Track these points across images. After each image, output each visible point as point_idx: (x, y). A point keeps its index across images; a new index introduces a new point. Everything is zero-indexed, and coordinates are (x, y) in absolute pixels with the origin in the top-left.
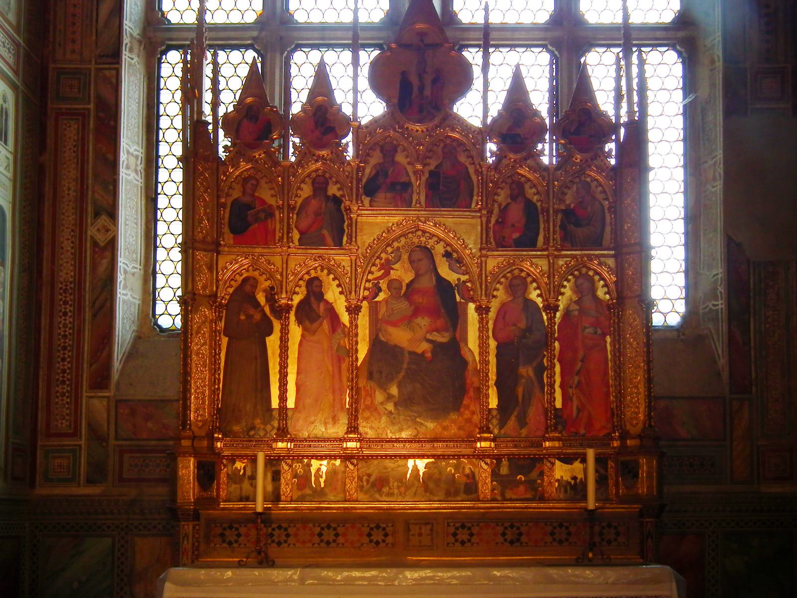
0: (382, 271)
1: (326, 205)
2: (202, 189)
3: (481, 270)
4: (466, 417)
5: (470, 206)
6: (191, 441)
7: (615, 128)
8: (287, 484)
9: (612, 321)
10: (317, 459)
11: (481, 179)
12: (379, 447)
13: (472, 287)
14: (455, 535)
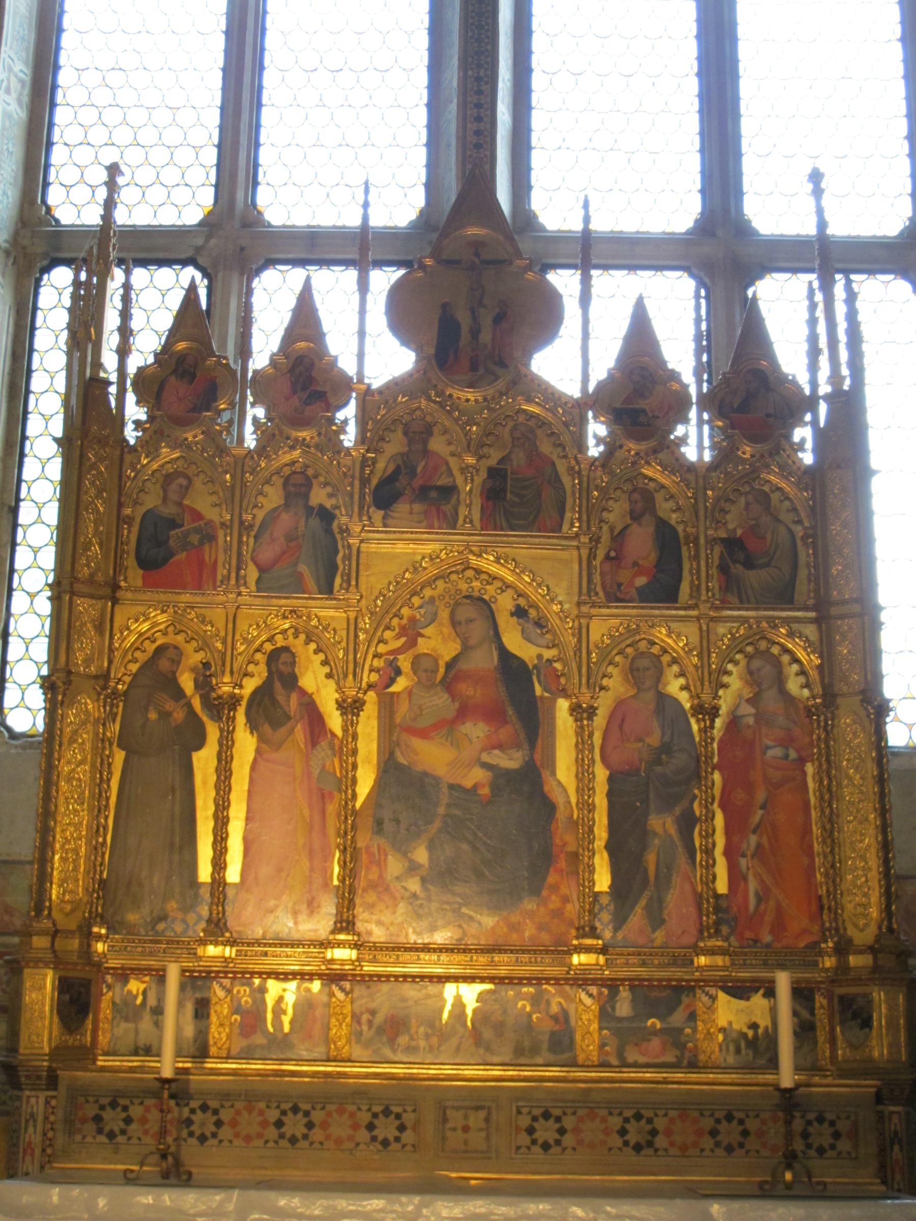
0: (403, 640)
1: (307, 521)
2: (93, 492)
3: (580, 641)
4: (552, 906)
5: (560, 530)
6: (49, 938)
7: (811, 403)
8: (221, 1025)
9: (815, 737)
10: (277, 978)
11: (579, 484)
12: (392, 960)
13: (564, 669)
14: (531, 1131)
